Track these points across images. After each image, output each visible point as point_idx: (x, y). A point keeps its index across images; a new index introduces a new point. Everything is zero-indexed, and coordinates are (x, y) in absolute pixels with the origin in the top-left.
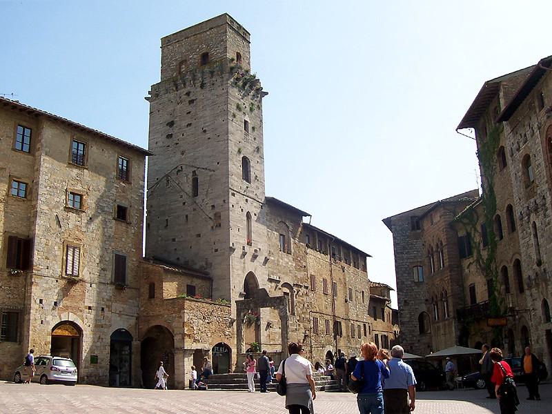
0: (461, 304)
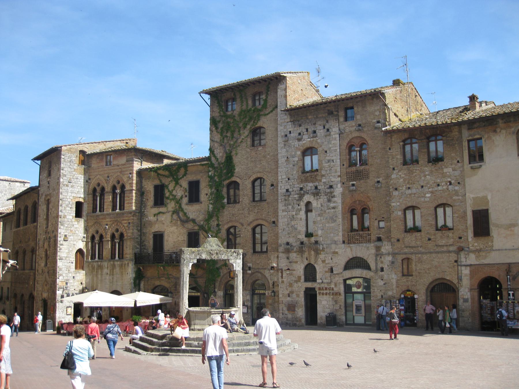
0: (138, 248)
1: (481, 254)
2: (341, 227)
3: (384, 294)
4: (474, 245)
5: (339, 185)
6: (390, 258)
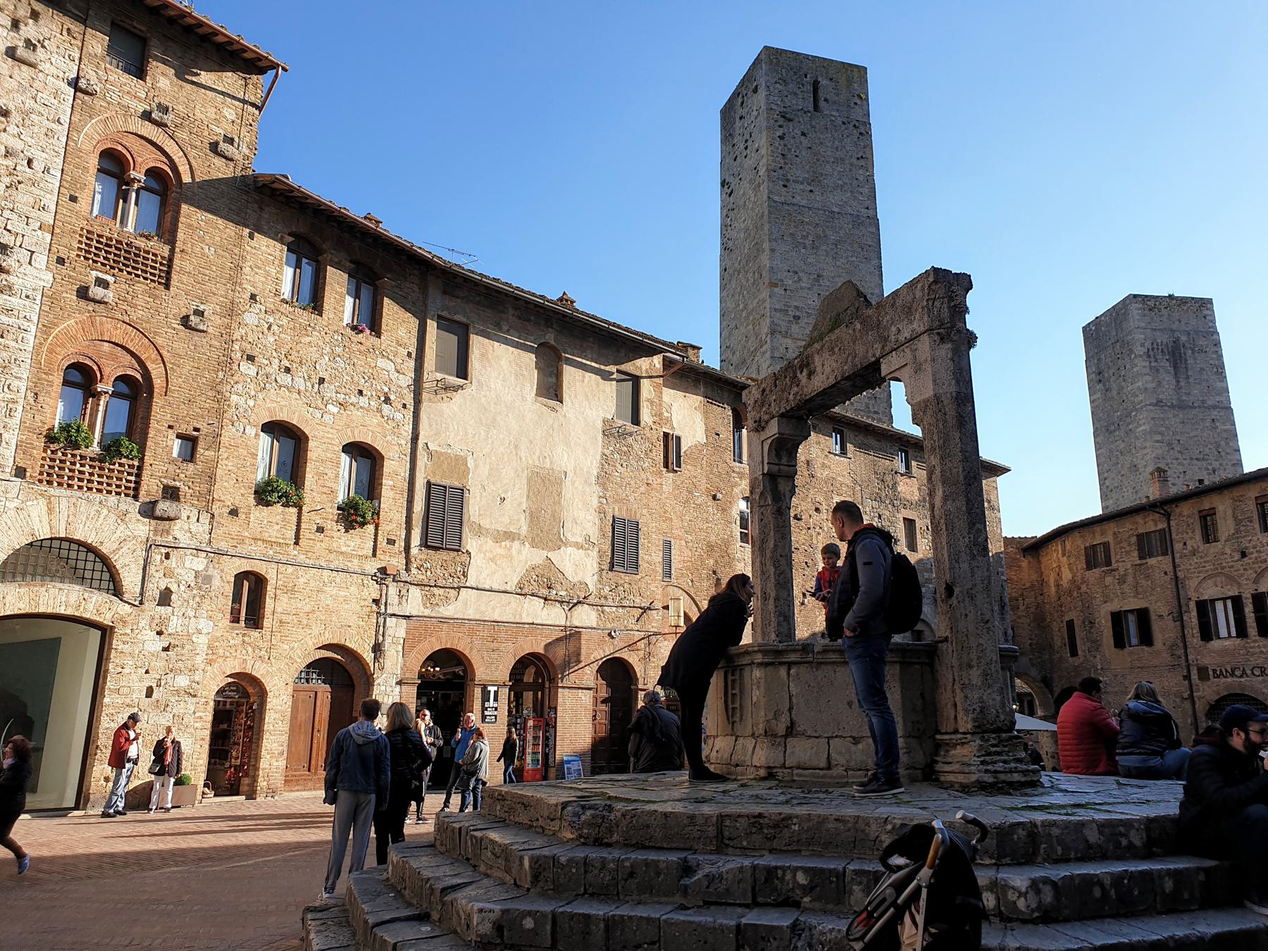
1: (435, 590)
2: (18, 415)
3: (158, 686)
4: (422, 566)
5: (41, 260)
6: (199, 563)
